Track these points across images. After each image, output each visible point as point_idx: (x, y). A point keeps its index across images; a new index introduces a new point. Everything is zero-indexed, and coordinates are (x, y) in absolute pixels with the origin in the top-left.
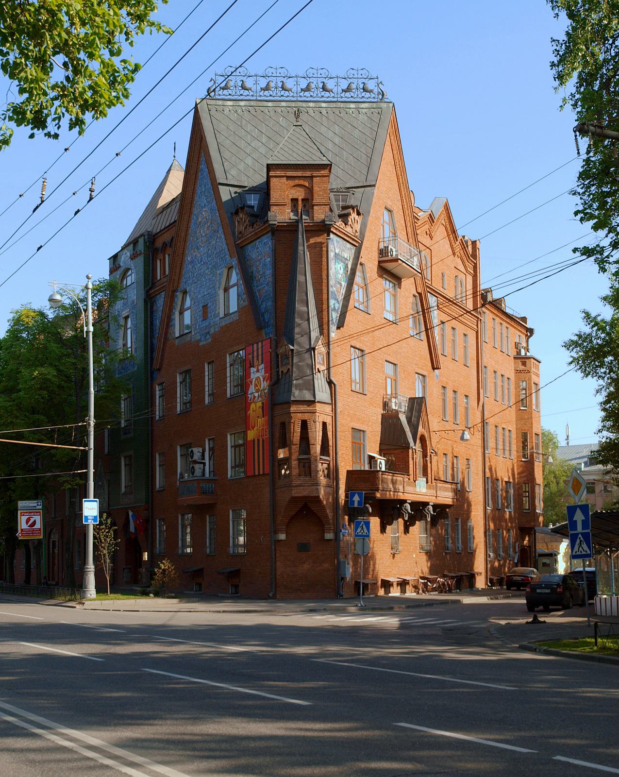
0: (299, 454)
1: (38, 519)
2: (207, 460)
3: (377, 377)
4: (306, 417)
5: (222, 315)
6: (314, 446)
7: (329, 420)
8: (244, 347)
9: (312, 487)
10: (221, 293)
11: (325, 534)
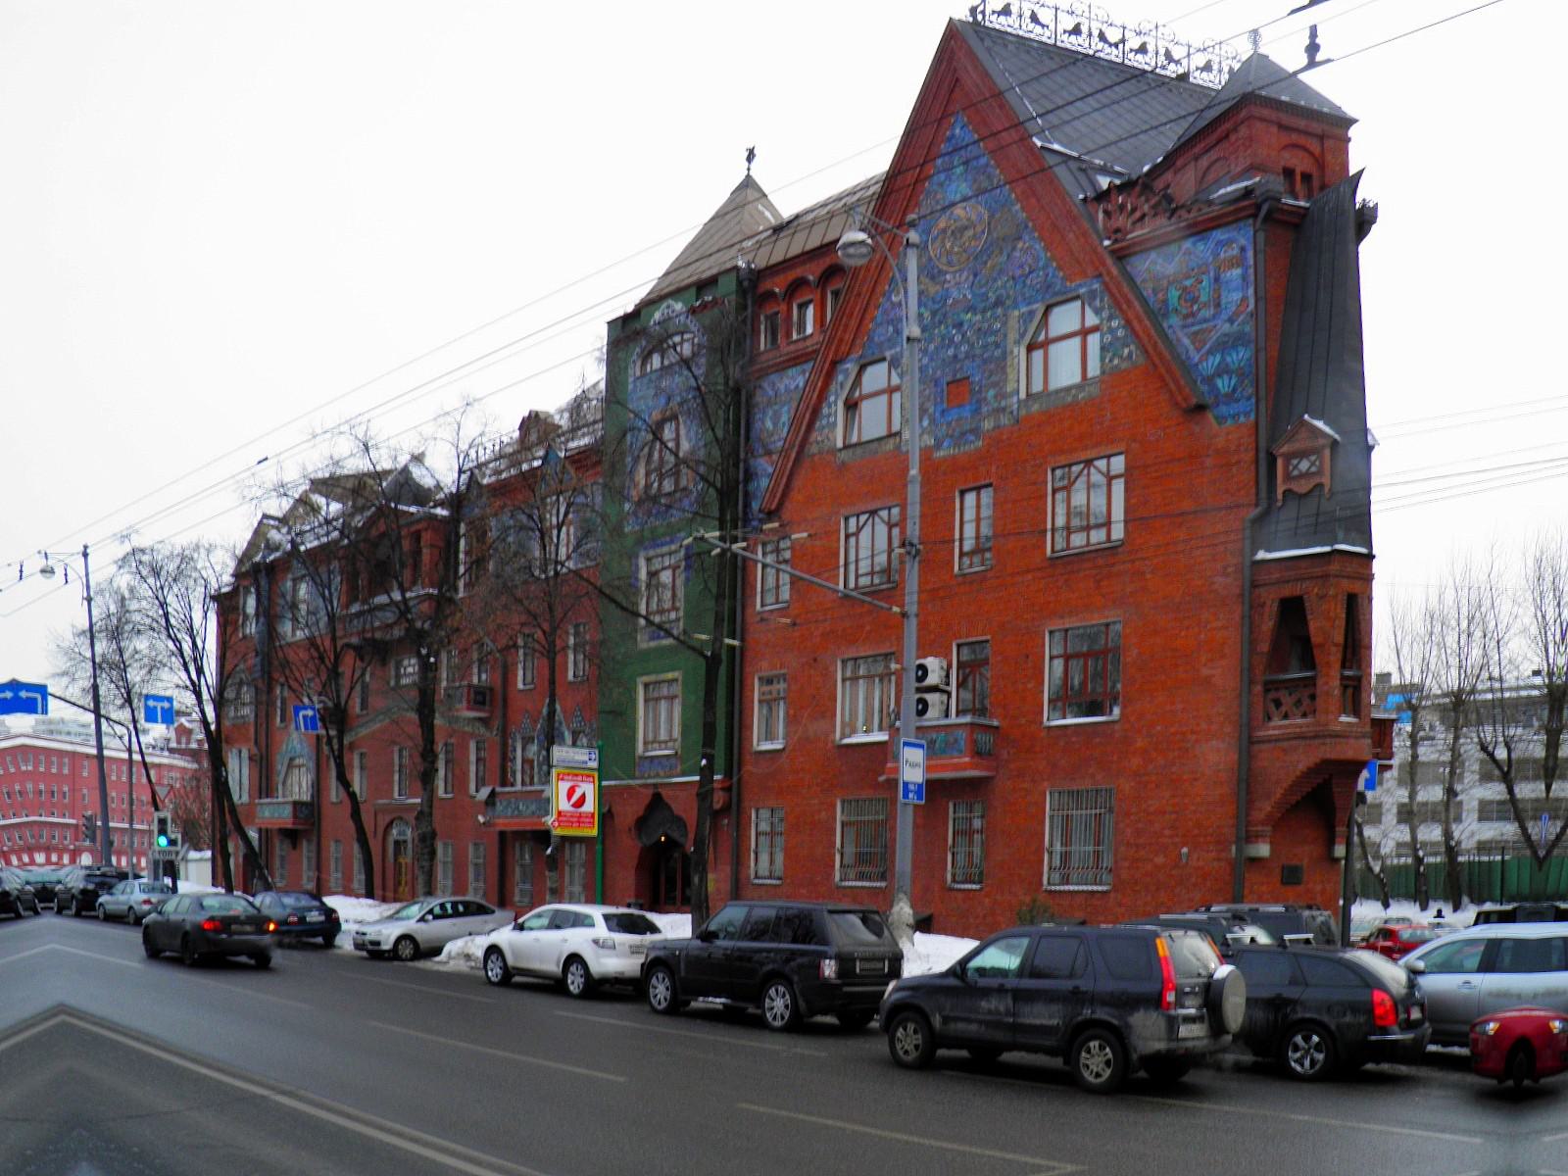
1: (588, 789)
2: (953, 688)
5: (1023, 395)
8: (1123, 449)
10: (1023, 351)
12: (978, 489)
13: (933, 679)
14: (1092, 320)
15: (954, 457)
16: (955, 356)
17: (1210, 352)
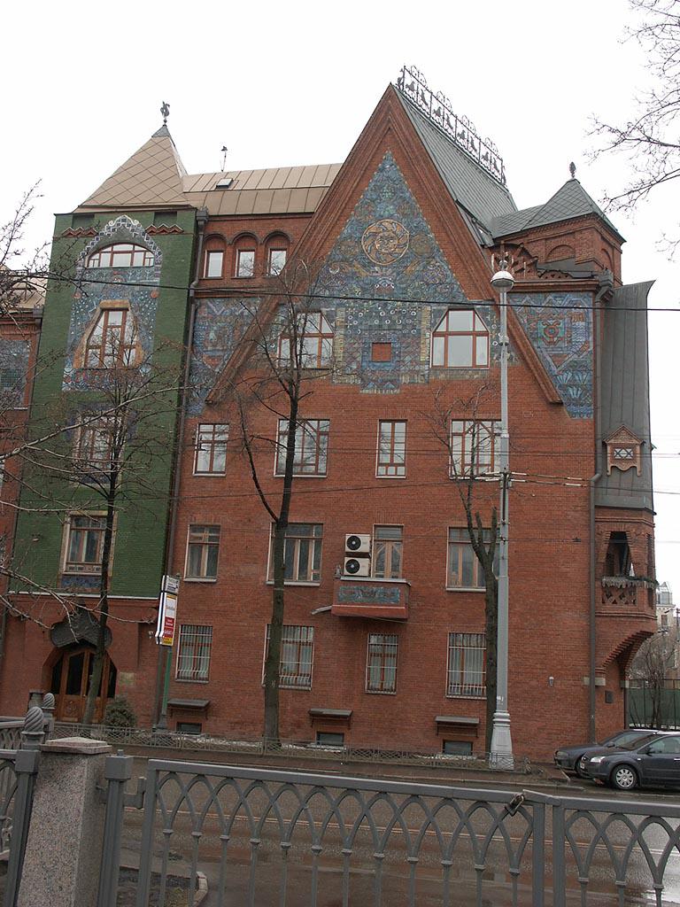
12: (393, 421)
13: (364, 548)
14: (480, 327)
15: (377, 396)
16: (380, 326)
17: (564, 371)
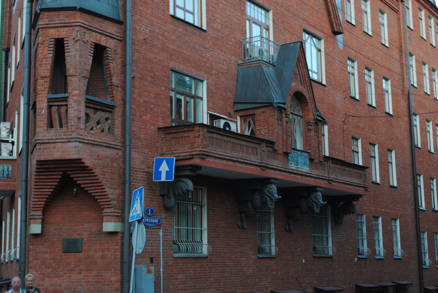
0: (49, 93)
3: (228, 13)
4: (63, 33)
6: (73, 79)
7: (111, 44)
9: (69, 144)
11: (104, 223)
